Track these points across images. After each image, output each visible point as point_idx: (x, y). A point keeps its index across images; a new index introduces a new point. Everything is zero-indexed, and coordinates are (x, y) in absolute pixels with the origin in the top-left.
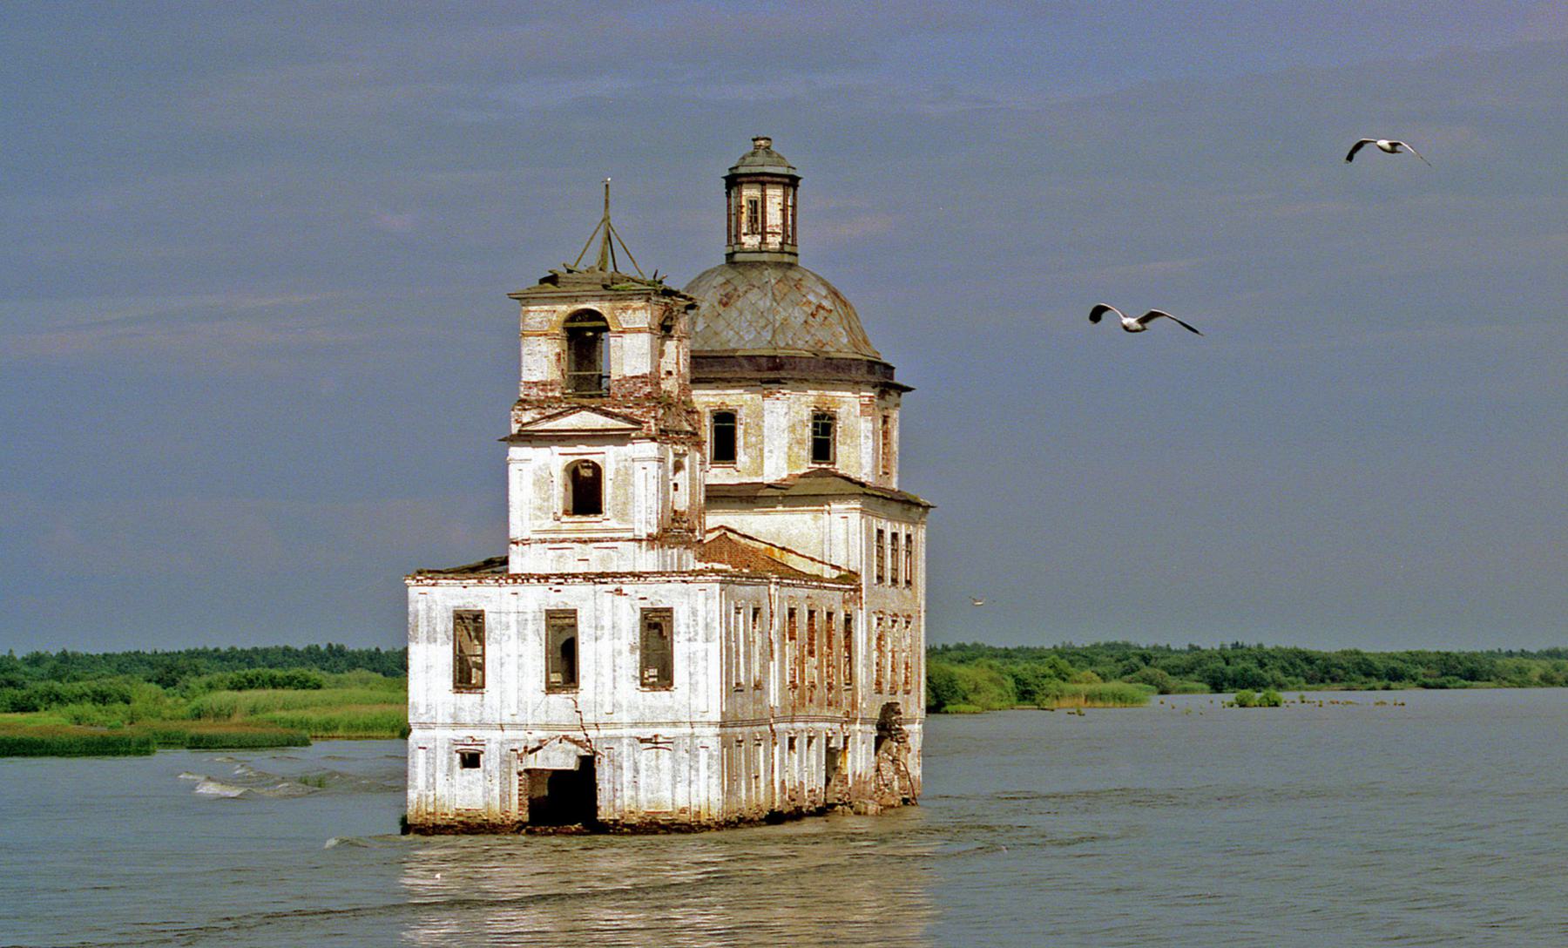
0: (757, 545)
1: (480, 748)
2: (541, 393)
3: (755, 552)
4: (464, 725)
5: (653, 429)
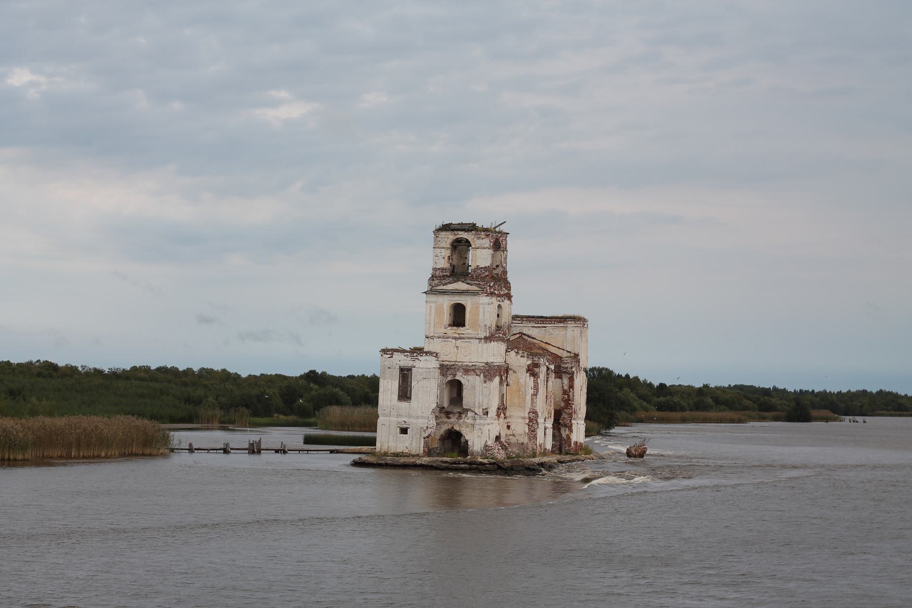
0: (535, 341)
1: (408, 426)
3: (534, 344)
5: (488, 291)
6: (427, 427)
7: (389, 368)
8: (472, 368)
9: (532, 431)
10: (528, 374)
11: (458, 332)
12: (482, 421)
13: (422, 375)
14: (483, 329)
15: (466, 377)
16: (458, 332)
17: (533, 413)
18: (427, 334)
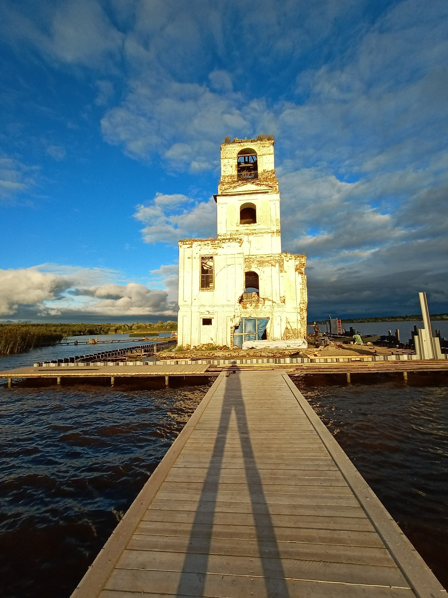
2: (229, 179)
10: (297, 273)
11: (250, 228)
12: (280, 309)
15: (261, 268)
16: (250, 228)
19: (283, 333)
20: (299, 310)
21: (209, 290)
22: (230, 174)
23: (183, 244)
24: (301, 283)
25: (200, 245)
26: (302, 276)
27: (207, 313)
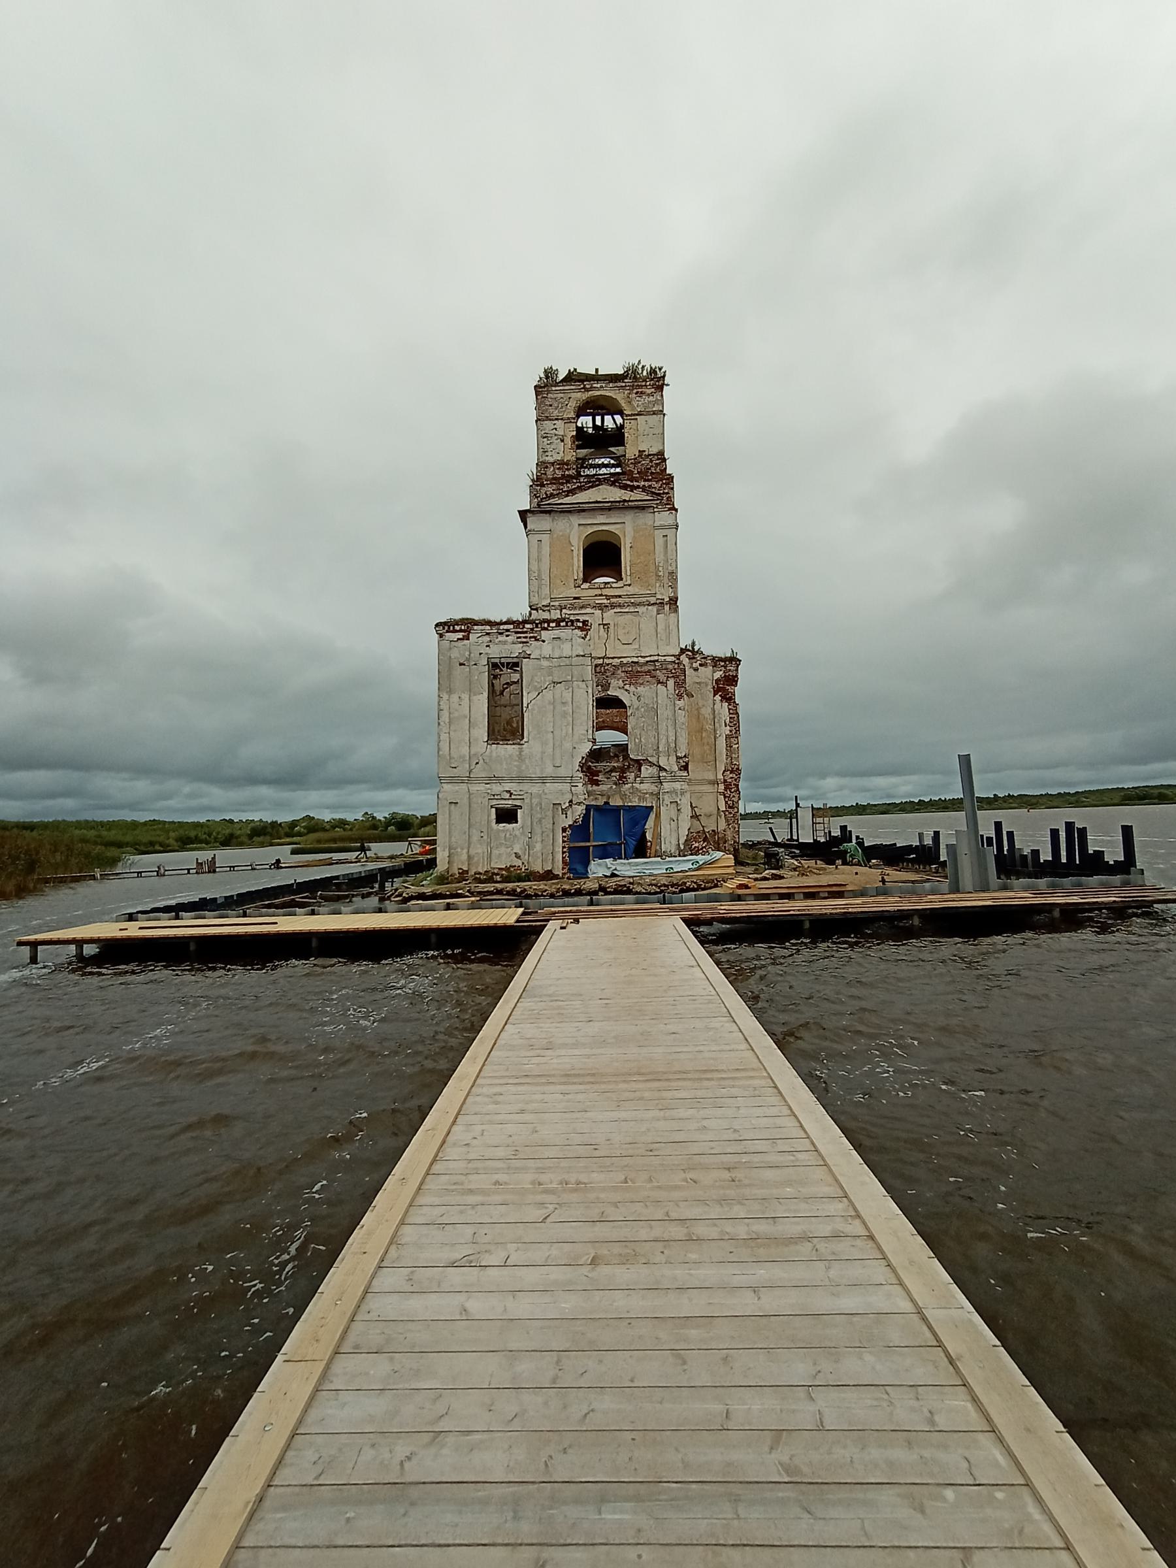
1: (518, 803)
4: (499, 780)
6: (571, 801)
7: (461, 664)
8: (646, 668)
9: (730, 807)
10: (718, 698)
13: (550, 674)
14: (666, 580)
15: (632, 688)
17: (732, 772)
18: (535, 600)
19: (682, 841)
20: (722, 787)
21: (511, 742)
22: (559, 459)
23: (447, 632)
24: (728, 722)
25: (488, 634)
26: (730, 707)
27: (507, 795)
